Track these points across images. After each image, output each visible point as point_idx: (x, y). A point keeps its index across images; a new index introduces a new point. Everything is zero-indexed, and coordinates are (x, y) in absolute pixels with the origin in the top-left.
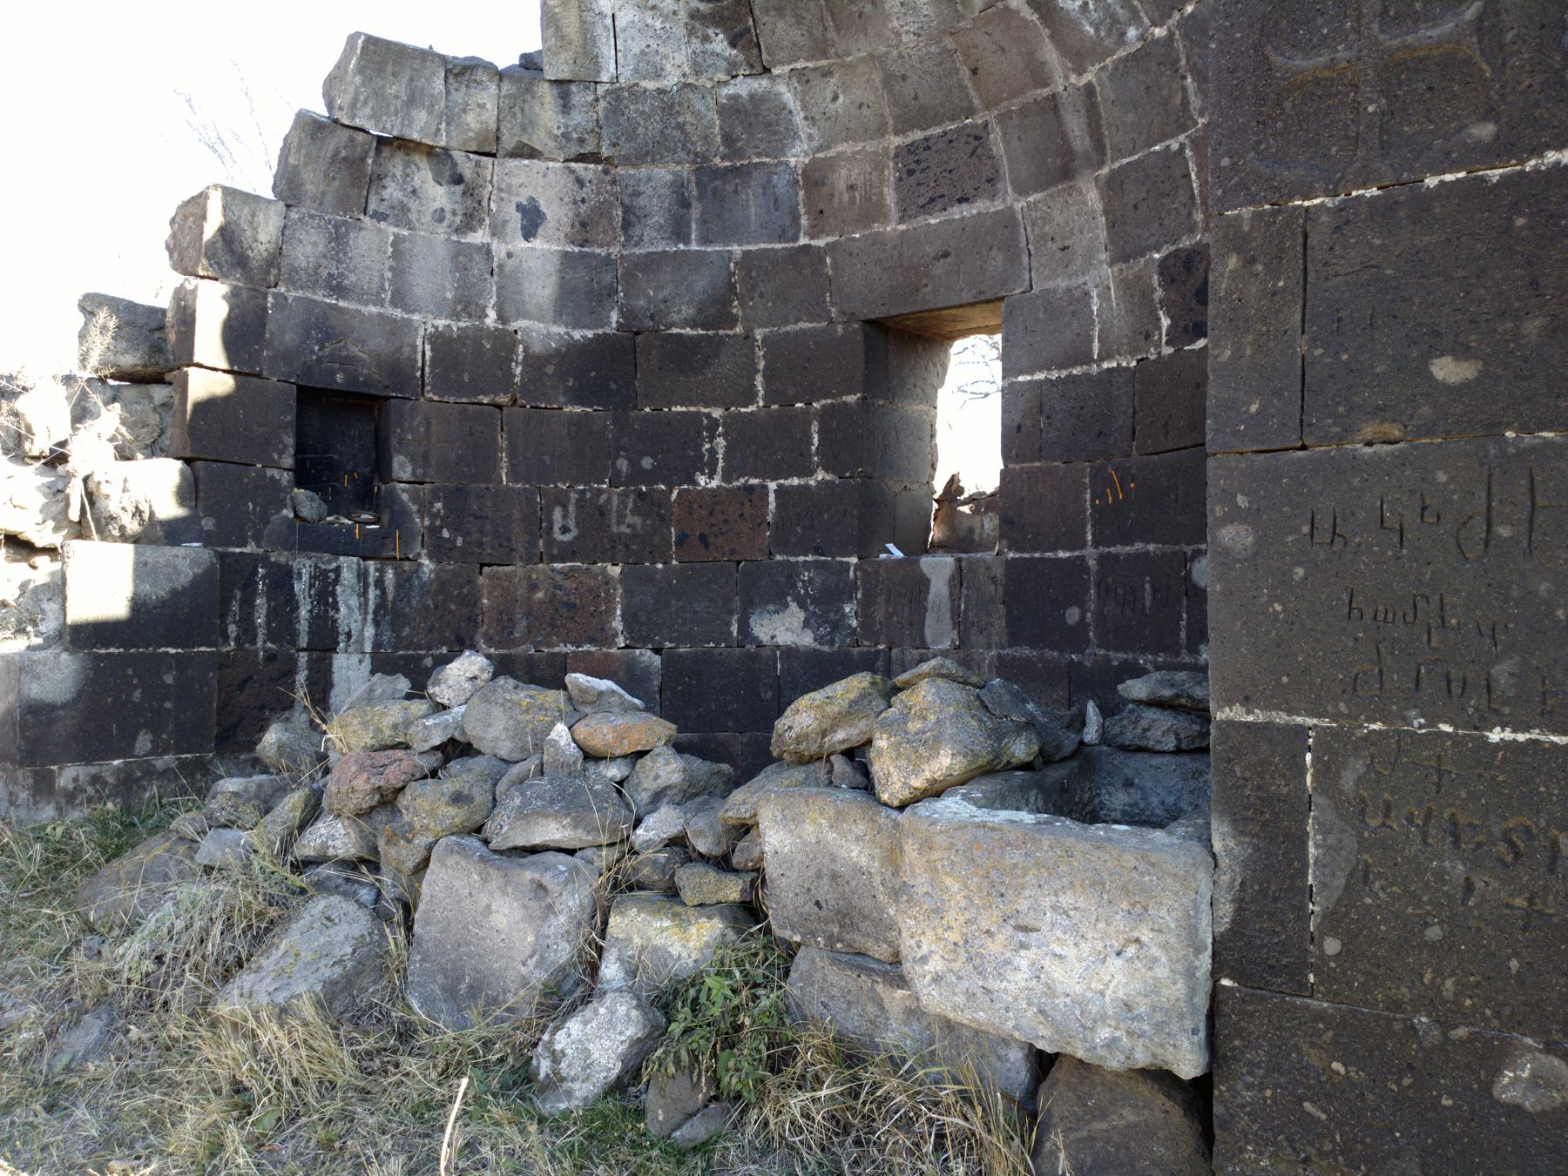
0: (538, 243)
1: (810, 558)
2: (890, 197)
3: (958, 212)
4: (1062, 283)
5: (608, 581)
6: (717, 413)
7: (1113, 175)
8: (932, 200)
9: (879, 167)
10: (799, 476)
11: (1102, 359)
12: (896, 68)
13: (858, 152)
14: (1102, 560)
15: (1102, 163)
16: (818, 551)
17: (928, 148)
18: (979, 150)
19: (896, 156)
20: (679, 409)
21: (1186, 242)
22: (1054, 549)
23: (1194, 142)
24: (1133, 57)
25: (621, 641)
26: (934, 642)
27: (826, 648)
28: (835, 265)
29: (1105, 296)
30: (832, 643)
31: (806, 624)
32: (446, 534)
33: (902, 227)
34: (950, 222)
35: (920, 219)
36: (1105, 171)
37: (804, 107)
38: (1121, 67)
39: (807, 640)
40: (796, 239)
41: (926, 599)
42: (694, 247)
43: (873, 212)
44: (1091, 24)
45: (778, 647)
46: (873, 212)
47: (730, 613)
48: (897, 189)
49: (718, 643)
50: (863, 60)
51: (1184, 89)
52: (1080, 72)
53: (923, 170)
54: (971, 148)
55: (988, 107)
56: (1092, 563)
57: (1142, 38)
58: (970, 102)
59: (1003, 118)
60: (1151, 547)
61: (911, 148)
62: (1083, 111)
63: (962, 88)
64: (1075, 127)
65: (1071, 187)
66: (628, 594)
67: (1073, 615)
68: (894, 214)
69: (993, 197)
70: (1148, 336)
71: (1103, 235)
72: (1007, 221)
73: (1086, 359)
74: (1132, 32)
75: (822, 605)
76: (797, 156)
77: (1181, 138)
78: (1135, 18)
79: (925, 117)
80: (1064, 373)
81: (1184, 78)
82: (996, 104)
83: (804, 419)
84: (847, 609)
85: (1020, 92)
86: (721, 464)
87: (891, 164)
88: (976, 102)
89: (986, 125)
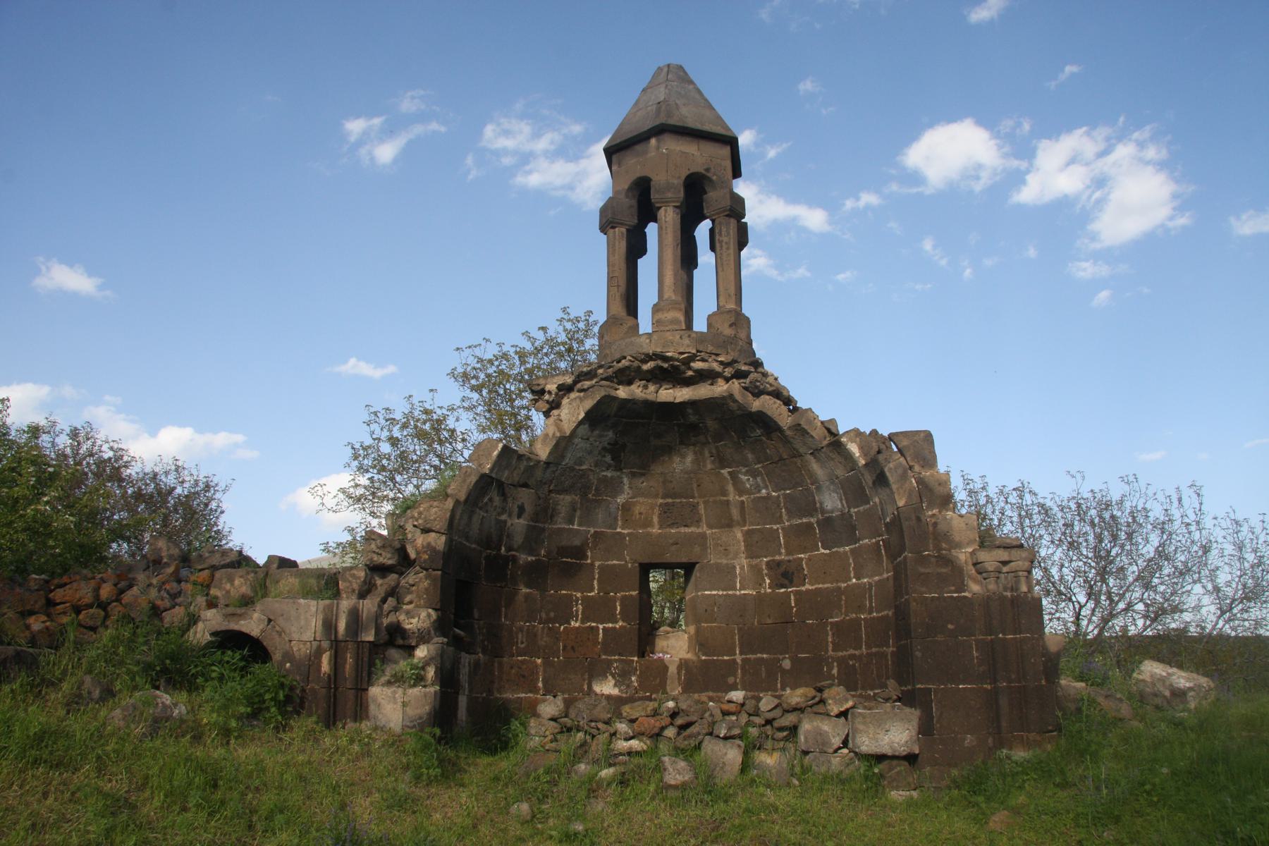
0: (521, 521)
1: (616, 657)
2: (655, 519)
3: (683, 530)
4: (724, 561)
5: (537, 666)
6: (579, 595)
7: (749, 531)
8: (673, 524)
9: (652, 508)
10: (612, 623)
11: (740, 590)
14: (743, 660)
15: (745, 526)
16: (620, 654)
20: (564, 592)
21: (777, 558)
22: (723, 656)
23: (783, 529)
25: (541, 692)
26: (671, 691)
27: (624, 695)
28: (630, 541)
29: (742, 568)
30: (627, 693)
31: (615, 685)
32: (486, 643)
33: (660, 531)
35: (668, 530)
36: (746, 528)
39: (615, 692)
40: (616, 529)
41: (667, 674)
42: (575, 527)
43: (650, 524)
45: (603, 695)
46: (648, 523)
47: (584, 680)
48: (659, 517)
49: (579, 693)
51: (781, 512)
55: (700, 497)
56: (739, 661)
59: (705, 503)
60: (765, 656)
61: (667, 504)
64: (735, 513)
66: (545, 671)
67: (731, 680)
68: (657, 526)
69: (698, 528)
70: (760, 585)
71: (743, 548)
72: (703, 536)
73: (736, 590)
74: (764, 491)
75: (621, 679)
76: (620, 500)
78: (766, 487)
79: (674, 496)
80: (725, 593)
83: (614, 600)
84: (633, 679)
86: (580, 616)
88: (696, 495)
89: (698, 503)
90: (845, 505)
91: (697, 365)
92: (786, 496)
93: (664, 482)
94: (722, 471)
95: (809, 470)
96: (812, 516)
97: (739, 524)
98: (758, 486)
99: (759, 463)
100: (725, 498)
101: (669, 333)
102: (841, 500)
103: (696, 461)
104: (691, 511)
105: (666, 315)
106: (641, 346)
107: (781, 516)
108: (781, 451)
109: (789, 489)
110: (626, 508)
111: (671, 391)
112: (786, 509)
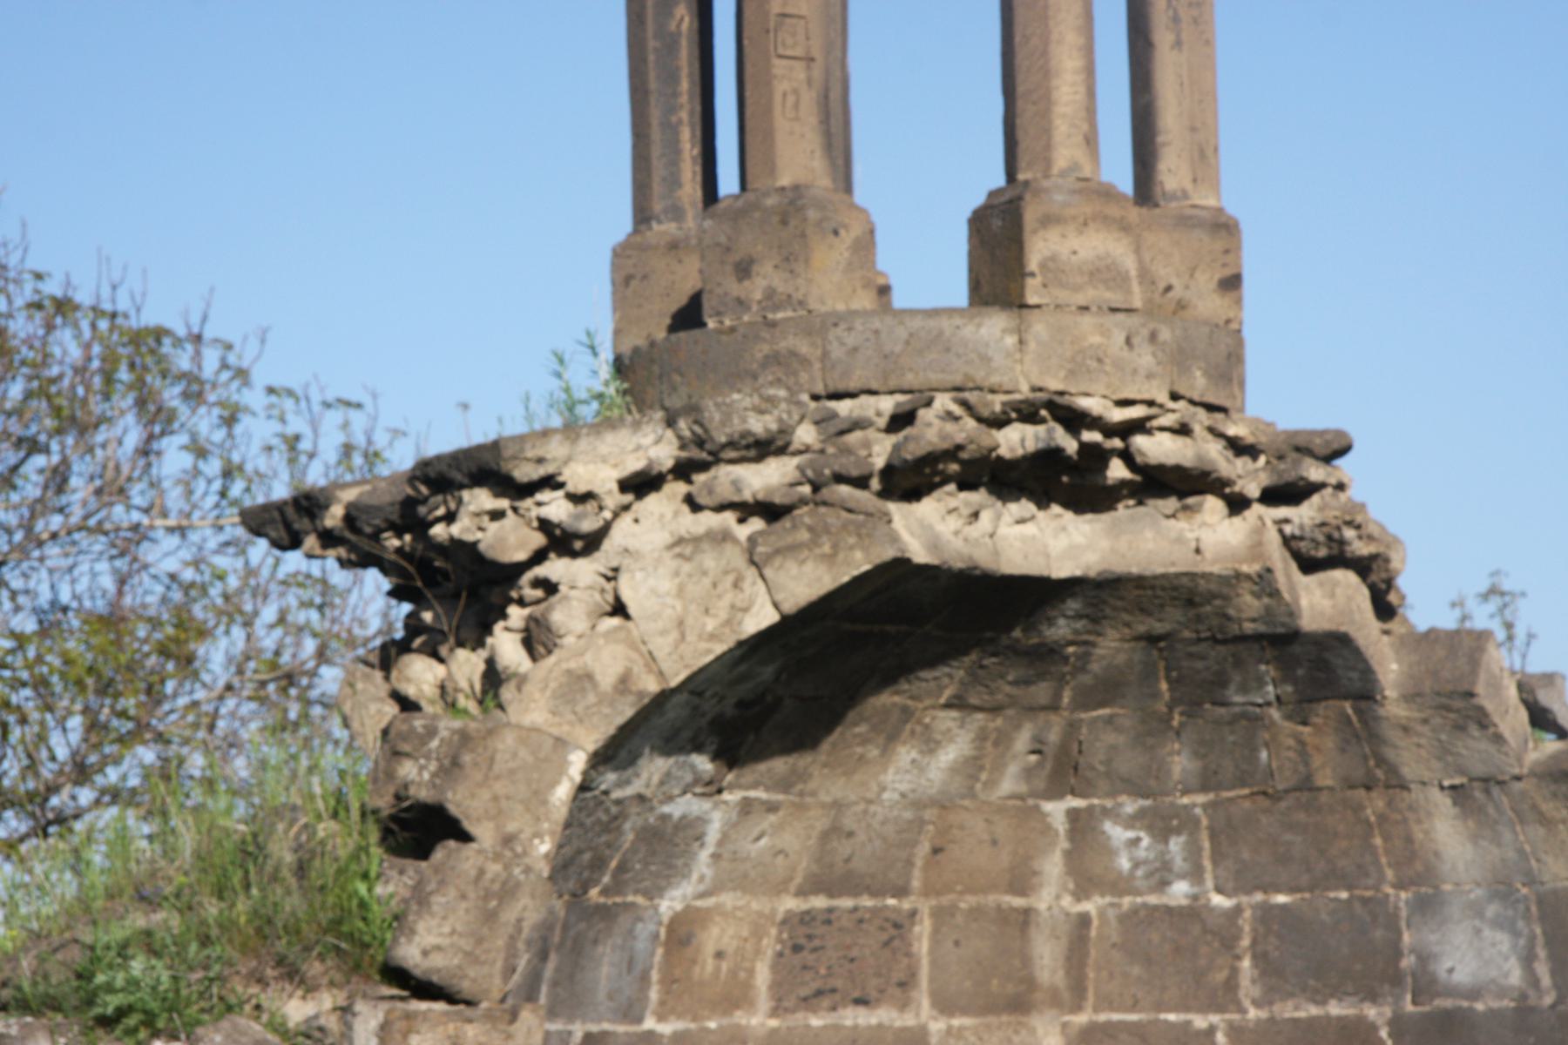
2: (763, 976)
3: (853, 1017)
8: (819, 993)
12: (848, 822)
13: (740, 908)
15: (1077, 1008)
17: (828, 922)
18: (896, 943)
19: (784, 922)
24: (1168, 910)
33: (773, 1023)
34: (837, 1028)
37: (720, 843)
38: (1142, 913)
40: (639, 1020)
44: (1131, 859)
46: (736, 997)
48: (775, 968)
50: (823, 806)
51: (1234, 972)
52: (1080, 894)
53: (815, 950)
54: (884, 937)
55: (927, 892)
57: (1195, 898)
58: (908, 882)
59: (939, 915)
61: (806, 918)
62: (1064, 941)
63: (909, 863)
64: (1047, 959)
65: (1020, 1023)
68: (764, 1001)
69: (903, 1006)
74: (1180, 890)
77: (1215, 1018)
78: (1196, 874)
81: (1238, 958)
82: (938, 893)
85: (985, 890)
87: (774, 931)
88: (916, 883)
89: (913, 913)
90: (1546, 980)
91: (1157, 448)
92: (1266, 914)
93: (825, 836)
94: (1048, 806)
95: (1409, 840)
96: (1373, 997)
97: (1055, 1001)
98: (1166, 866)
99: (1204, 789)
100: (1018, 902)
101: (1087, 321)
102: (1528, 960)
103: (971, 768)
104: (887, 944)
105: (1074, 242)
106: (986, 359)
107: (1231, 985)
108: (1317, 761)
109: (1291, 890)
110: (681, 934)
111: (1029, 529)
112: (1260, 958)
